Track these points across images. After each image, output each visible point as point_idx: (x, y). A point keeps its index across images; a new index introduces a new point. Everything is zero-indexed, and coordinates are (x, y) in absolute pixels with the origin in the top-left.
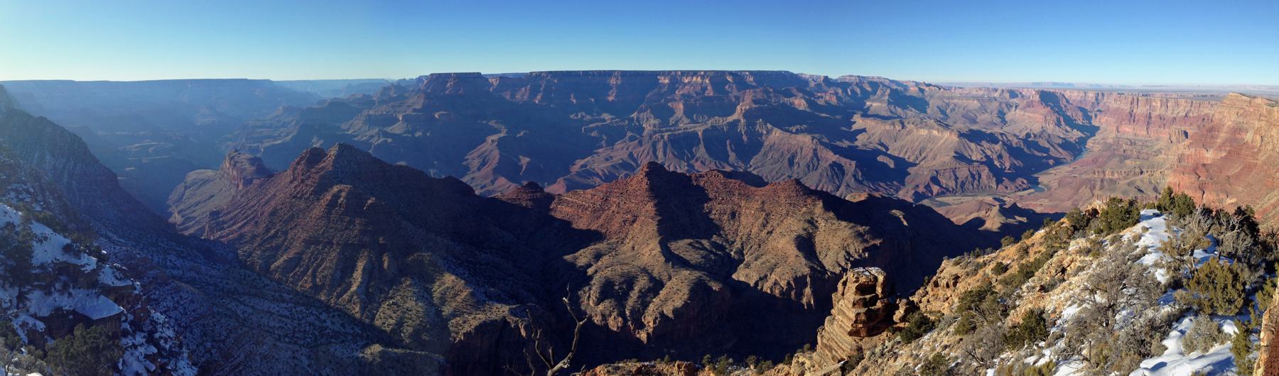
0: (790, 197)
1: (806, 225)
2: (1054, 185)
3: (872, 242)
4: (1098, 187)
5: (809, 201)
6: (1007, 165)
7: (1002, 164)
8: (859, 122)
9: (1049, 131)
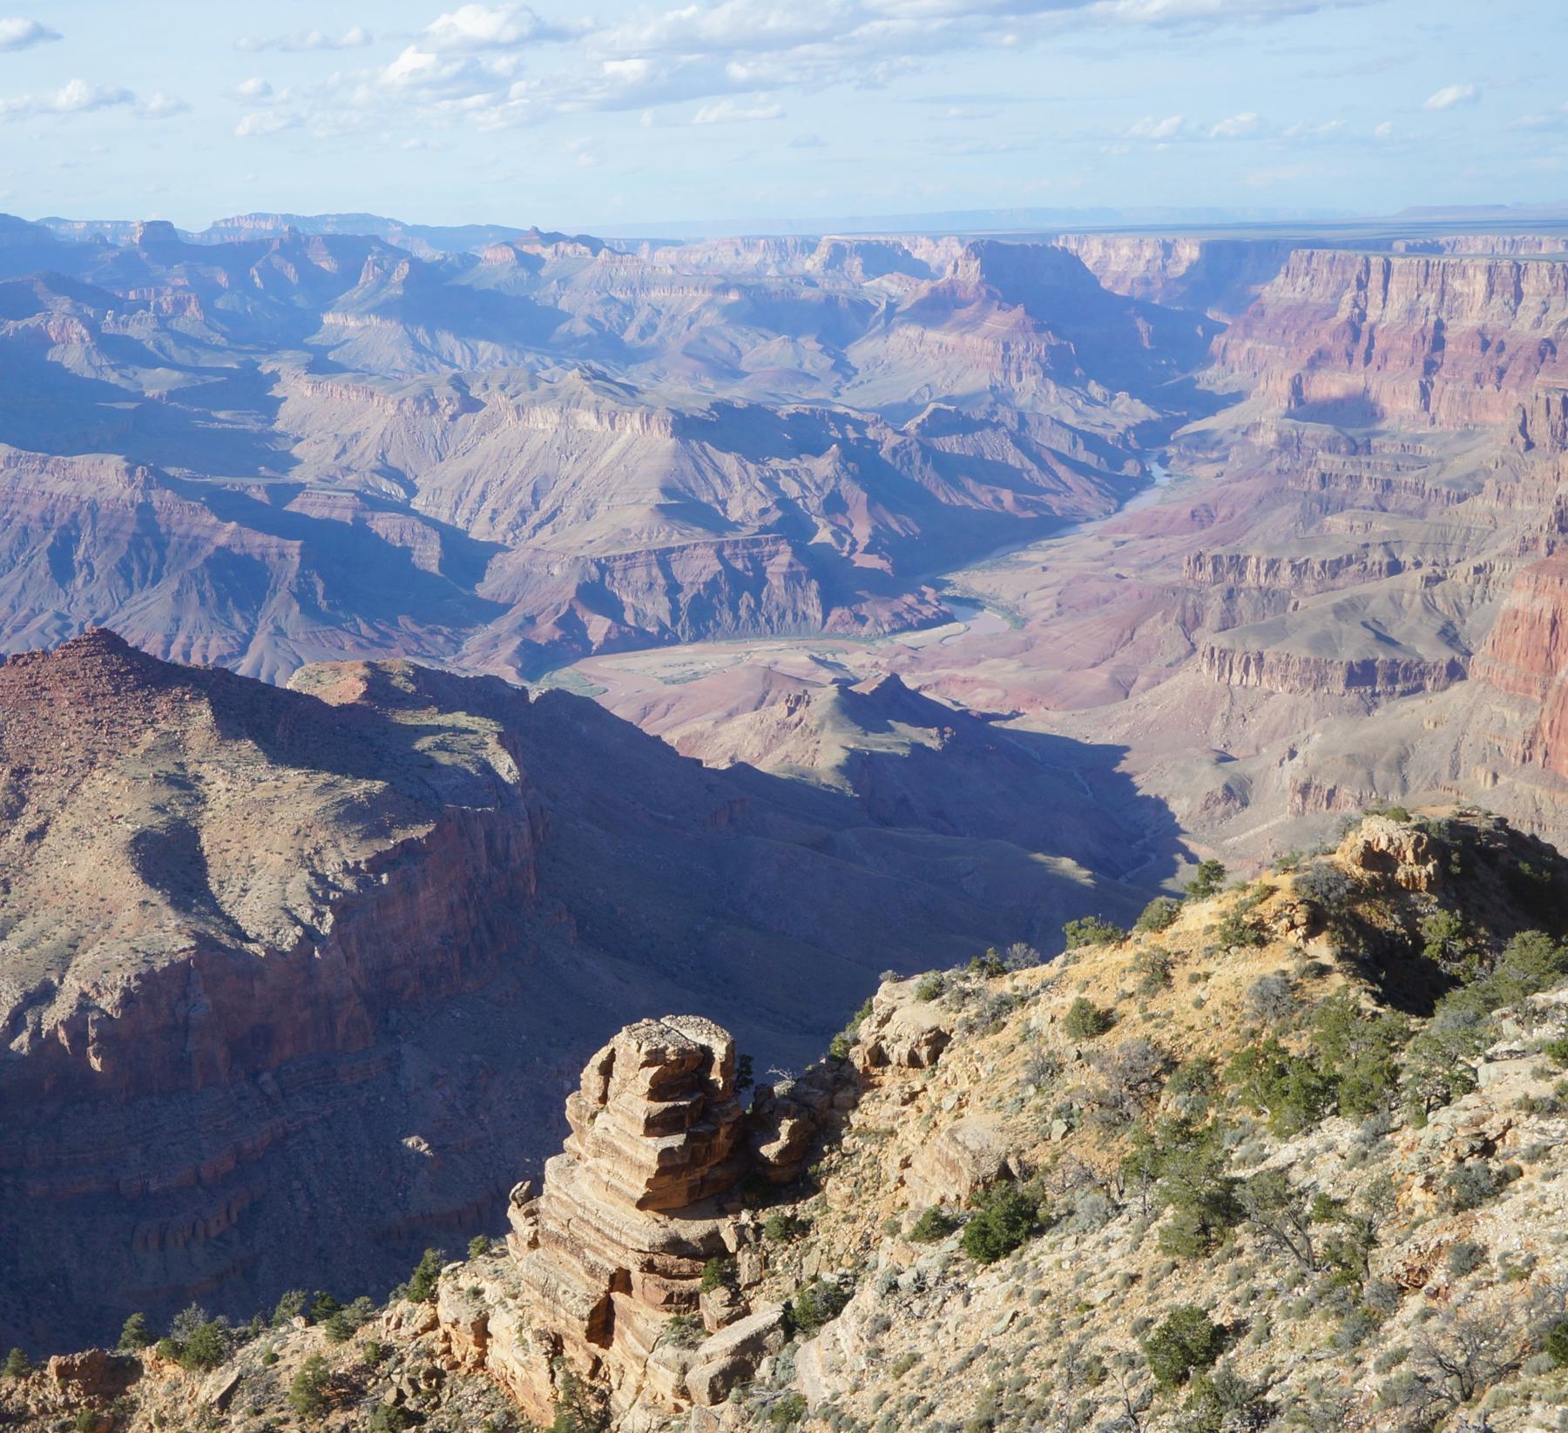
0: (89, 698)
1: (164, 794)
2: (1040, 605)
3: (400, 836)
4: (1212, 619)
5: (162, 704)
6: (862, 532)
7: (840, 533)
8: (299, 395)
9: (1023, 401)
